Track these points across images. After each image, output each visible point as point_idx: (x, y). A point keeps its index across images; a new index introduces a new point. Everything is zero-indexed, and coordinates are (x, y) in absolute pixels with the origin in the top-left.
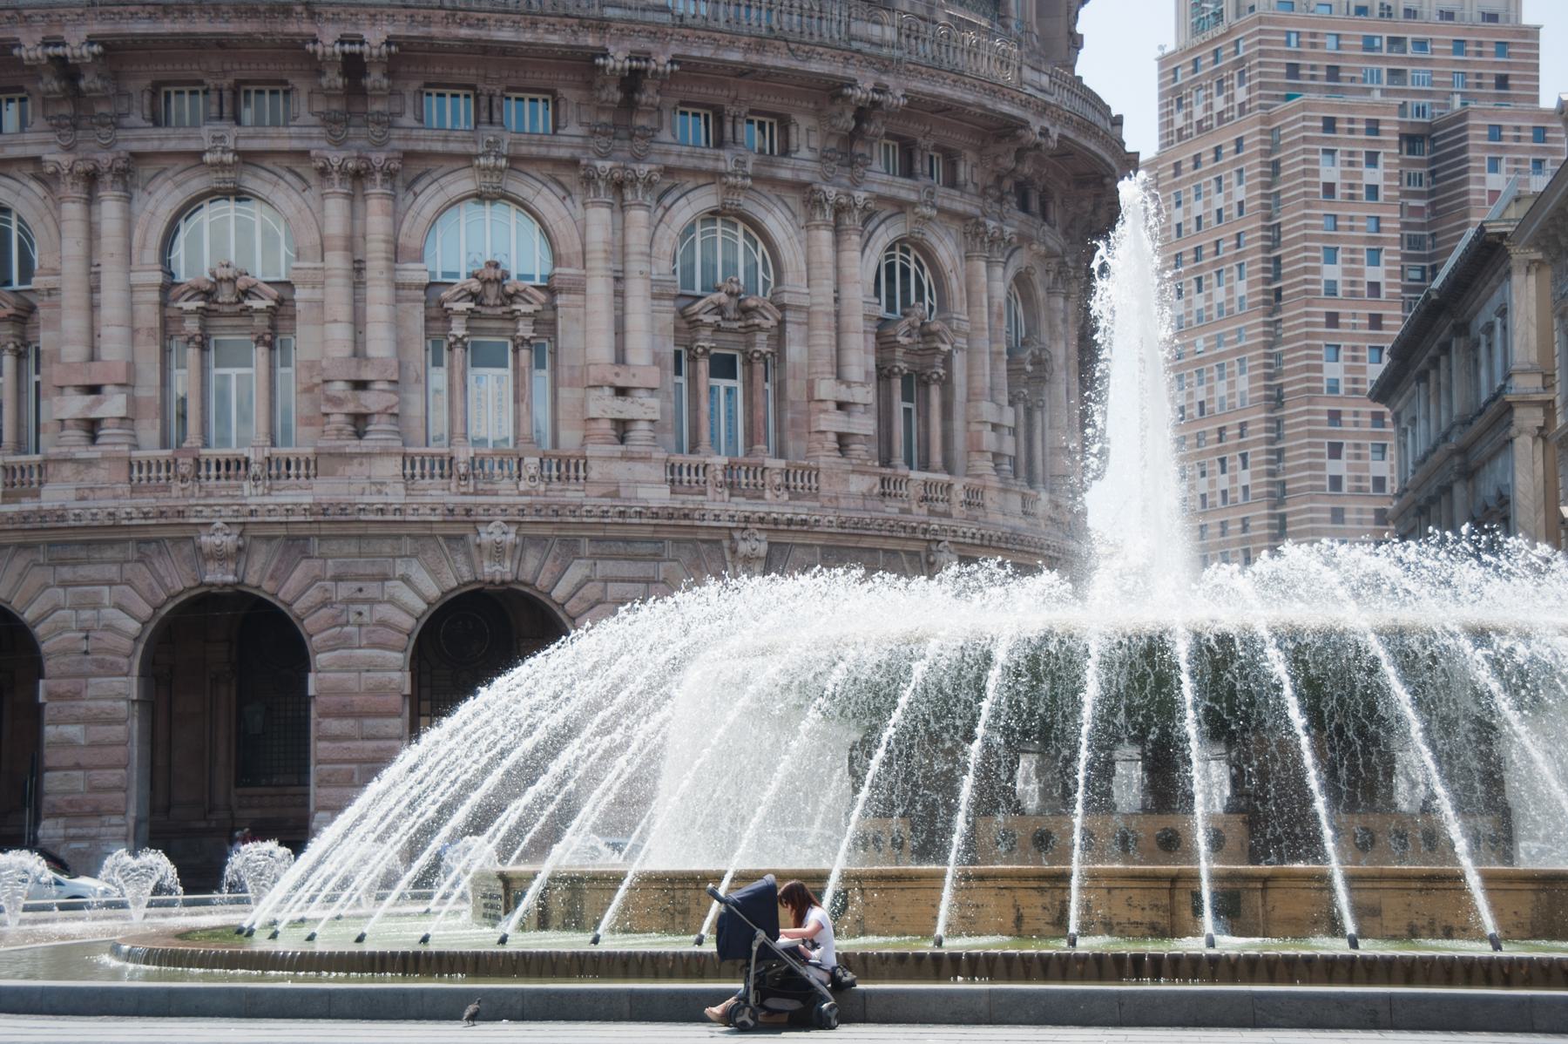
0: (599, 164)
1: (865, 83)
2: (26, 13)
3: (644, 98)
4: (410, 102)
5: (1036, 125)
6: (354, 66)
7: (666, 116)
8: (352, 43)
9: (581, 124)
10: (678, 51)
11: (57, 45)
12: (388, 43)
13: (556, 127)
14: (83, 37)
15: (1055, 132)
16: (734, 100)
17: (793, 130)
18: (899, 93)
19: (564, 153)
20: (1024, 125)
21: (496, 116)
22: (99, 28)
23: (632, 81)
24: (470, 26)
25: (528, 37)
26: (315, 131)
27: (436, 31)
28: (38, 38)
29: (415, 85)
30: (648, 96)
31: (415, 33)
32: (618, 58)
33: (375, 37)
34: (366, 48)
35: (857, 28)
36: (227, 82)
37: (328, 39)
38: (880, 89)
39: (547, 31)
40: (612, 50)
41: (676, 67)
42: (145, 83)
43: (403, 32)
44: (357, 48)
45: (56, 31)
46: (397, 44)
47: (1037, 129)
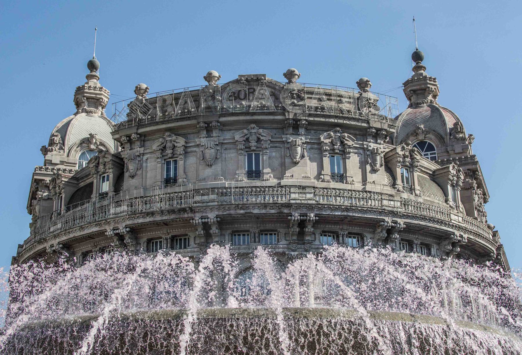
0: (293, 253)
1: (388, 220)
2: (108, 221)
3: (307, 229)
4: (227, 237)
5: (457, 233)
6: (206, 226)
7: (317, 236)
8: (205, 219)
9: (286, 240)
10: (318, 213)
11: (117, 229)
12: (217, 218)
13: (278, 242)
14: (124, 226)
15: (466, 236)
16: (342, 229)
17: (365, 238)
18: (402, 223)
19: (281, 250)
20: (454, 234)
21: (257, 240)
22: (128, 222)
23: (302, 224)
24: (243, 209)
25: (264, 211)
26: (196, 249)
27: (232, 212)
28: (112, 228)
29: (229, 231)
30: (309, 229)
31: (225, 213)
32: (296, 216)
33: (212, 216)
34: (209, 220)
35: (385, 202)
36: (168, 237)
37: (197, 219)
38: (396, 222)
39: (270, 209)
40: (293, 213)
41: (317, 218)
42: (145, 239)
43: (221, 213)
44: (206, 220)
45: (116, 225)
46: (220, 218)
47: (458, 235)
